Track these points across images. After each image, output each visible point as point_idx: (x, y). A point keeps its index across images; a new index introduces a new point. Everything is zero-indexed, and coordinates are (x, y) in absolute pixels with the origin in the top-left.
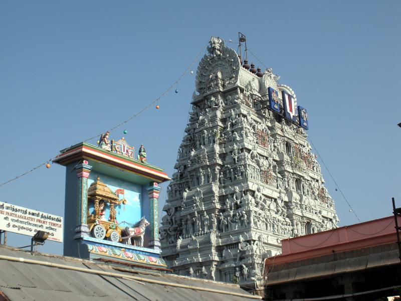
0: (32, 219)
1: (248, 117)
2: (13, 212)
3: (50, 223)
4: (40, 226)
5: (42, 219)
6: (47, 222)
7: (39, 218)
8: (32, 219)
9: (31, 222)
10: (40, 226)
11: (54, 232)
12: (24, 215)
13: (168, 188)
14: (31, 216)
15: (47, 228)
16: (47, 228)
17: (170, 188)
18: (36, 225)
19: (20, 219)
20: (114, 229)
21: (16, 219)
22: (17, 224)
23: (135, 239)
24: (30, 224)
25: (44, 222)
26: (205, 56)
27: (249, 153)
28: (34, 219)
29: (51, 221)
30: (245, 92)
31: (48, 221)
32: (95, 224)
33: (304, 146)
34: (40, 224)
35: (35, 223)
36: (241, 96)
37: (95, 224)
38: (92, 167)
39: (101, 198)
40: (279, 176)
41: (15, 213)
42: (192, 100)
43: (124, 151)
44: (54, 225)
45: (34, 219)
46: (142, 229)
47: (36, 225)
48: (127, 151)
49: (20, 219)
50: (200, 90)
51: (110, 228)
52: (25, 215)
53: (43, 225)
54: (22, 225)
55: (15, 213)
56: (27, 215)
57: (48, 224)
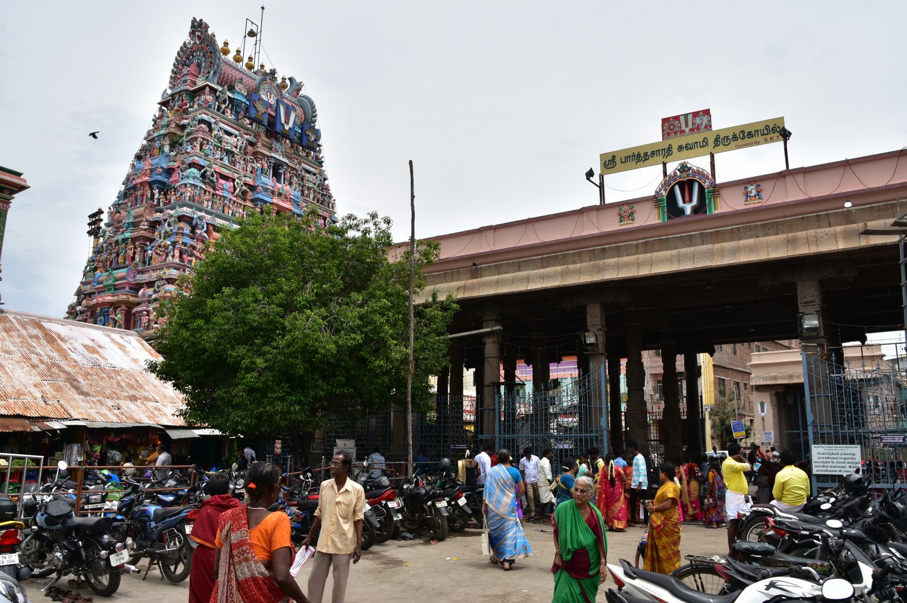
1: (213, 125)
26: (185, 44)
27: (200, 170)
30: (218, 93)
33: (314, 174)
36: (210, 98)
40: (249, 204)
42: (160, 100)
50: (173, 85)
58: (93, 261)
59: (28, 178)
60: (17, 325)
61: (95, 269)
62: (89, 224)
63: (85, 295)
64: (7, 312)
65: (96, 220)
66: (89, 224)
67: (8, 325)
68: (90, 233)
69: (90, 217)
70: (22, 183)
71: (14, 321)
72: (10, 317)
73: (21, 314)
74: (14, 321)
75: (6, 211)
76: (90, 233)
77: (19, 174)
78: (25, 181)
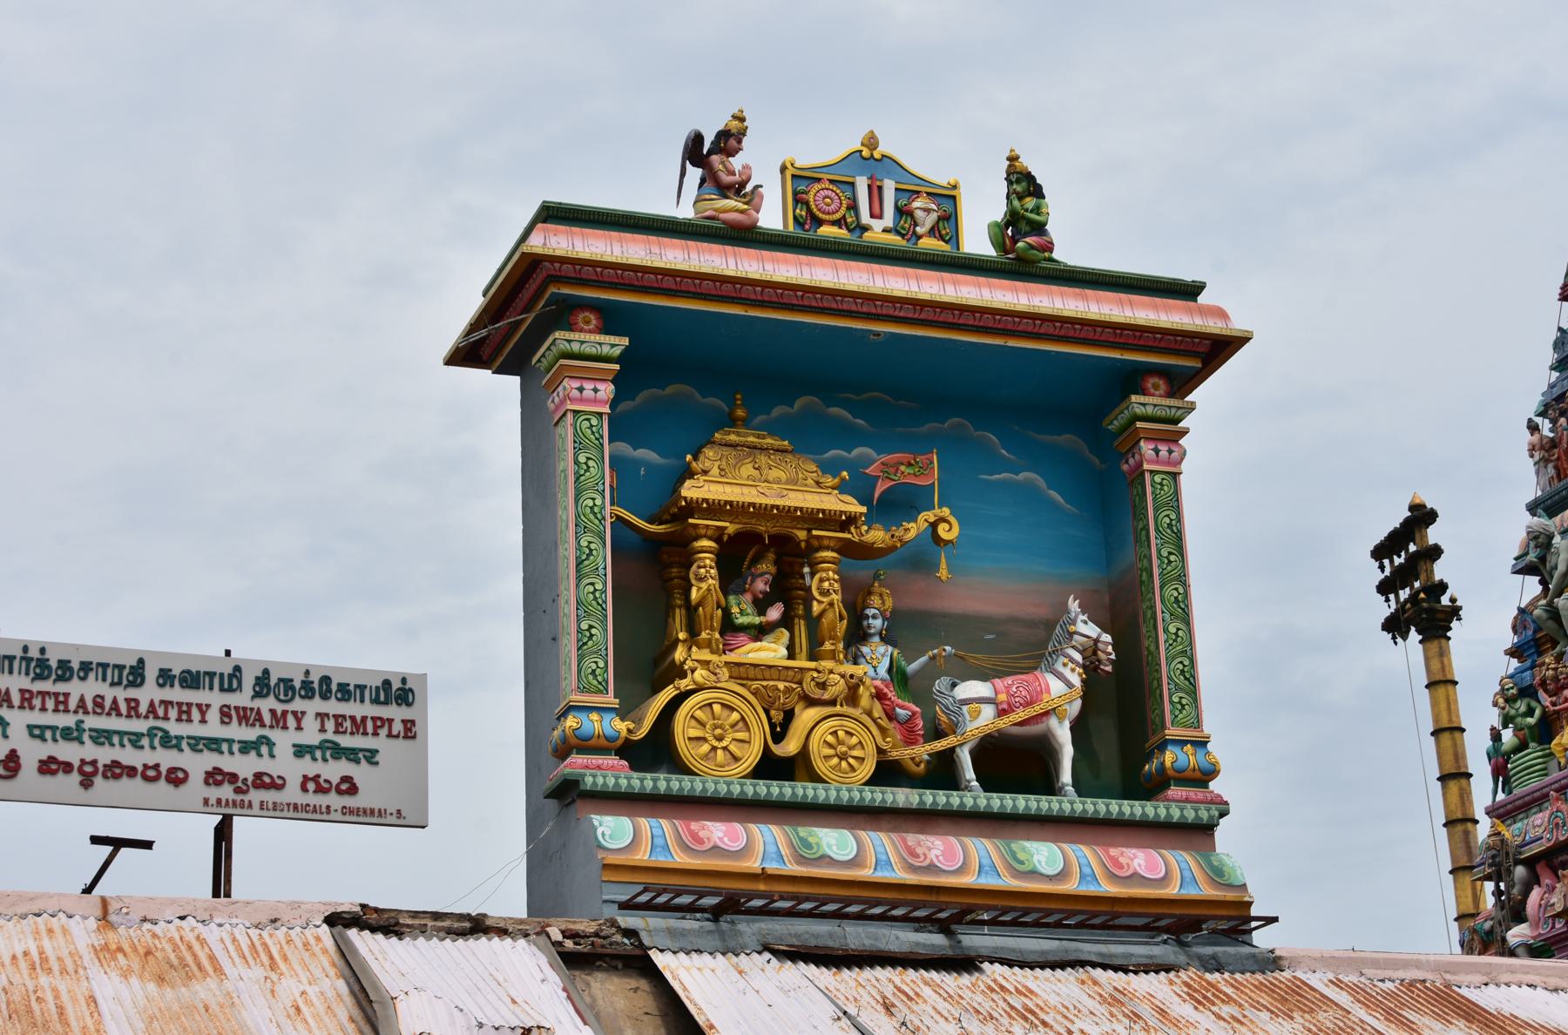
0: (184, 712)
2: (46, 686)
3: (322, 716)
4: (246, 747)
5: (267, 705)
6: (299, 716)
7: (243, 699)
8: (184, 712)
9: (174, 728)
10: (246, 747)
11: (360, 772)
12: (121, 694)
13: (1533, 428)
14: (177, 694)
15: (300, 751)
16: (300, 751)
17: (1545, 426)
18: (214, 744)
19: (92, 722)
20: (833, 703)
21: (67, 720)
22: (68, 752)
23: (1015, 761)
24: (168, 741)
25: (279, 720)
28: (203, 709)
29: (333, 707)
31: (317, 705)
32: (684, 684)
34: (251, 734)
35: (214, 728)
37: (684, 684)
38: (625, 341)
39: (731, 528)
41: (61, 687)
43: (877, 214)
44: (359, 726)
45: (203, 709)
46: (1061, 686)
47: (214, 744)
48: (902, 212)
49: (92, 722)
51: (811, 702)
52: (132, 693)
53: (275, 735)
54: (105, 755)
55: (61, 687)
56: (148, 693)
57: (310, 723)
58: (1527, 692)
59: (1230, 300)
60: (1360, 1012)
61: (1546, 730)
62: (1385, 588)
63: (1530, 863)
64: (1295, 962)
65: (1412, 559)
66: (1435, 552)
67: (1325, 1018)
68: (1395, 626)
69: (1380, 553)
70: (1213, 326)
71: (1343, 998)
72: (1317, 980)
73: (1356, 962)
74: (1343, 998)
75: (1175, 476)
76: (1395, 626)
77: (1188, 291)
78: (1221, 314)
